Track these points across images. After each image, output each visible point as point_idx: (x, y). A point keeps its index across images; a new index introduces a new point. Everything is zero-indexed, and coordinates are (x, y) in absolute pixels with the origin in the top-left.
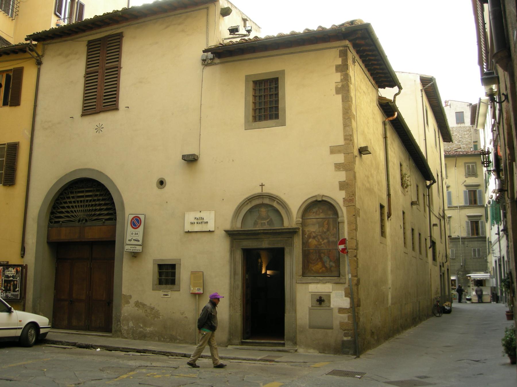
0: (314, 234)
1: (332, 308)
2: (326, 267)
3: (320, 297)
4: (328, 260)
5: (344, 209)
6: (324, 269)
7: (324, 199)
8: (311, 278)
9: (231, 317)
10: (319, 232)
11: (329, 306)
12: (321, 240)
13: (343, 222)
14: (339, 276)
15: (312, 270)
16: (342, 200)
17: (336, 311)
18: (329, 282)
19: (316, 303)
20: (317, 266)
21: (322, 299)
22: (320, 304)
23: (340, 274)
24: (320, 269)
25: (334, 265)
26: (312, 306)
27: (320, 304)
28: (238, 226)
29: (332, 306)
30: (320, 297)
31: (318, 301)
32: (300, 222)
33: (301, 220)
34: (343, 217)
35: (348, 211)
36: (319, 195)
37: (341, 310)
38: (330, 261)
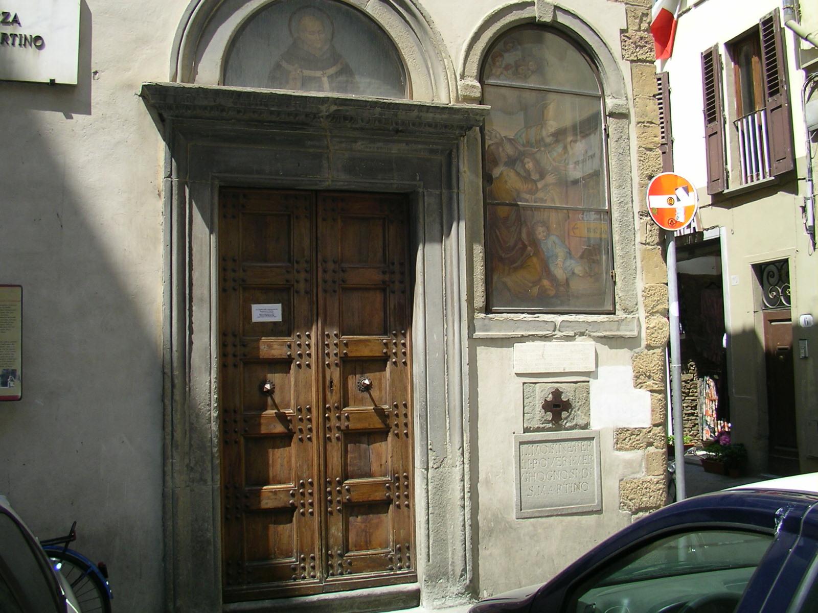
0: (509, 150)
1: (599, 432)
3: (557, 394)
4: (560, 252)
7: (562, 19)
9: (168, 501)
11: (586, 426)
17: (608, 441)
18: (582, 334)
19: (538, 415)
21: (564, 398)
22: (557, 418)
25: (578, 270)
26: (526, 430)
27: (557, 418)
28: (208, 75)
29: (595, 426)
30: (557, 394)
31: (547, 406)
37: (625, 437)
38: (569, 254)
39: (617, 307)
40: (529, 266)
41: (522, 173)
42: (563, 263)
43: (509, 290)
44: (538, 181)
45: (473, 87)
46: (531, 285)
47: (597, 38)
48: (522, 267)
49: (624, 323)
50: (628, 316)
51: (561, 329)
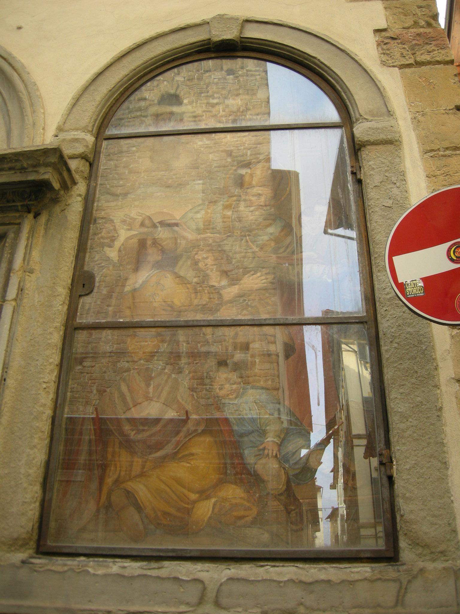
2: (250, 479)
5: (391, 81)
6: (233, 493)
7: (254, 33)
8: (115, 567)
10: (208, 226)
12: (215, 280)
13: (392, 143)
14: (389, 556)
15: (129, 494)
16: (371, 40)
20: (179, 470)
23: (392, 535)
24: (204, 494)
32: (80, 149)
33: (90, 139)
34: (390, 113)
35: (411, 88)
36: (221, 18)
39: (403, 543)
40: (193, 454)
41: (190, 275)
42: (280, 445)
43: (139, 508)
44: (224, 287)
45: (76, 140)
46: (193, 496)
47: (327, 46)
48: (174, 456)
49: (418, 583)
50: (430, 566)
51: (224, 601)
